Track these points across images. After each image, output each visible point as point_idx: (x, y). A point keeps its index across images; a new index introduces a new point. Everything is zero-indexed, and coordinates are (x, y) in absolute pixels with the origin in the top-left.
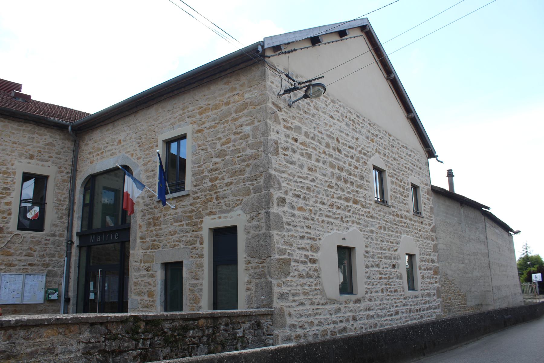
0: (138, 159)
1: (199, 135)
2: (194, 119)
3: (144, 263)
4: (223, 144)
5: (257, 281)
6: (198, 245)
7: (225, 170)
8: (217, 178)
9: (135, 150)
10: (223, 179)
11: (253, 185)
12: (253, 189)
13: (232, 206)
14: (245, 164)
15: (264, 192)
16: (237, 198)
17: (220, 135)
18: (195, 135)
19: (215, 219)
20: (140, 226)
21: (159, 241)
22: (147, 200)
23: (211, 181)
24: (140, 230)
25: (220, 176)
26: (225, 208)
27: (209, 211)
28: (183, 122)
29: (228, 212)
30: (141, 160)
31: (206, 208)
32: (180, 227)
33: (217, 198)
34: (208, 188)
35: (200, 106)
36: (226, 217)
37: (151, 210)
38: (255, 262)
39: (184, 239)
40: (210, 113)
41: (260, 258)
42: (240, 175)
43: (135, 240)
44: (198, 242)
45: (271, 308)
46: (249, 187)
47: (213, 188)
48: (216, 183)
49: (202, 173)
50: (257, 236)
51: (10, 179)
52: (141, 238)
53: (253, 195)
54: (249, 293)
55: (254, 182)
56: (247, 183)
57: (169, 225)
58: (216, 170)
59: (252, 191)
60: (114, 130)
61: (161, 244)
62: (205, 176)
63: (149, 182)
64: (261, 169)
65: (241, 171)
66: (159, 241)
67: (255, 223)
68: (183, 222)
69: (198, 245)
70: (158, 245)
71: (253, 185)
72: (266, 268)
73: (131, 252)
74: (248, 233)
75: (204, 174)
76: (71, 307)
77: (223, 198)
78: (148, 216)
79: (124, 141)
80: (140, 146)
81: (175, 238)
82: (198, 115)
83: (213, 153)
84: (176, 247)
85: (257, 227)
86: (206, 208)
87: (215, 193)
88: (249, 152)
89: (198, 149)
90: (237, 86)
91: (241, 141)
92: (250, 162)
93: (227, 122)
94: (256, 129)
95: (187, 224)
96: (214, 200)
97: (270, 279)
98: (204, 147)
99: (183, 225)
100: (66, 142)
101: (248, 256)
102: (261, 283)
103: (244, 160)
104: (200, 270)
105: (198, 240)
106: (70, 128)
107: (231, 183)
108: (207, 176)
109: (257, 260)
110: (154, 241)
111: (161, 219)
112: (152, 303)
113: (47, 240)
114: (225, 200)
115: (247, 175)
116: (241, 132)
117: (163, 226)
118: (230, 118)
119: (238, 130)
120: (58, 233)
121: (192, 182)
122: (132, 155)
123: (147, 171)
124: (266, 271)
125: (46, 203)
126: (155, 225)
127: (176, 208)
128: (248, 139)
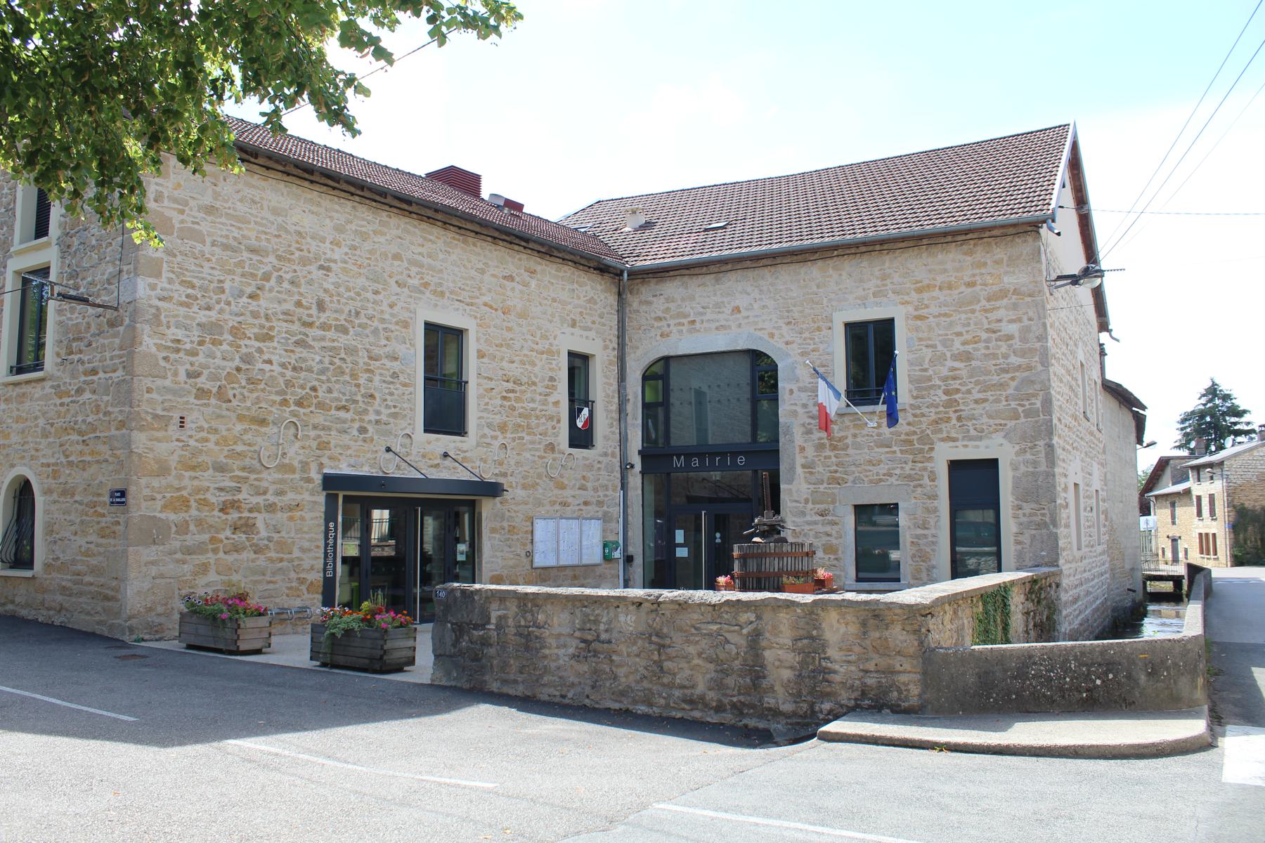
0: (787, 343)
1: (919, 323)
2: (906, 298)
4: (964, 344)
5: (1033, 532)
7: (973, 380)
8: (958, 391)
9: (779, 328)
11: (1023, 406)
12: (1023, 411)
13: (986, 431)
14: (1010, 375)
15: (1042, 417)
16: (997, 422)
17: (959, 329)
18: (910, 322)
20: (802, 449)
23: (946, 393)
25: (964, 389)
26: (973, 432)
27: (945, 435)
28: (885, 299)
29: (980, 438)
30: (794, 346)
31: (940, 431)
33: (959, 419)
35: (918, 279)
36: (977, 447)
38: (1027, 508)
40: (936, 293)
41: (1037, 502)
43: (792, 469)
44: (926, 478)
45: (1058, 566)
47: (948, 404)
48: (957, 396)
49: (930, 381)
51: (554, 362)
52: (804, 466)
53: (1023, 420)
54: (1019, 547)
55: (1026, 403)
56: (1012, 403)
57: (866, 450)
58: (954, 378)
62: (934, 385)
64: (1038, 386)
65: (1001, 385)
67: (1028, 456)
69: (926, 481)
71: (1023, 406)
72: (1048, 515)
74: (1015, 469)
76: (637, 569)
77: (971, 419)
79: (747, 309)
80: (789, 323)
81: (883, 469)
82: (913, 292)
83: (948, 354)
85: (1035, 464)
87: (956, 411)
88: (1015, 360)
90: (989, 261)
91: (999, 343)
92: (1017, 374)
93: (973, 311)
94: (1025, 331)
96: (954, 421)
97: (1054, 531)
98: (930, 342)
99: (895, 452)
100: (607, 295)
101: (1017, 499)
102: (1041, 534)
103: (1007, 372)
105: (926, 474)
106: (625, 275)
107: (985, 400)
108: (940, 387)
109: (1034, 506)
110: (836, 472)
111: (849, 441)
112: (836, 562)
113: (599, 462)
114: (974, 422)
115: (1010, 391)
116: (1000, 331)
117: (850, 451)
118: (977, 307)
119: (994, 326)
120: (610, 452)
121: (910, 391)
122: (772, 335)
124: (1047, 520)
125: (467, 382)
128: (1011, 342)
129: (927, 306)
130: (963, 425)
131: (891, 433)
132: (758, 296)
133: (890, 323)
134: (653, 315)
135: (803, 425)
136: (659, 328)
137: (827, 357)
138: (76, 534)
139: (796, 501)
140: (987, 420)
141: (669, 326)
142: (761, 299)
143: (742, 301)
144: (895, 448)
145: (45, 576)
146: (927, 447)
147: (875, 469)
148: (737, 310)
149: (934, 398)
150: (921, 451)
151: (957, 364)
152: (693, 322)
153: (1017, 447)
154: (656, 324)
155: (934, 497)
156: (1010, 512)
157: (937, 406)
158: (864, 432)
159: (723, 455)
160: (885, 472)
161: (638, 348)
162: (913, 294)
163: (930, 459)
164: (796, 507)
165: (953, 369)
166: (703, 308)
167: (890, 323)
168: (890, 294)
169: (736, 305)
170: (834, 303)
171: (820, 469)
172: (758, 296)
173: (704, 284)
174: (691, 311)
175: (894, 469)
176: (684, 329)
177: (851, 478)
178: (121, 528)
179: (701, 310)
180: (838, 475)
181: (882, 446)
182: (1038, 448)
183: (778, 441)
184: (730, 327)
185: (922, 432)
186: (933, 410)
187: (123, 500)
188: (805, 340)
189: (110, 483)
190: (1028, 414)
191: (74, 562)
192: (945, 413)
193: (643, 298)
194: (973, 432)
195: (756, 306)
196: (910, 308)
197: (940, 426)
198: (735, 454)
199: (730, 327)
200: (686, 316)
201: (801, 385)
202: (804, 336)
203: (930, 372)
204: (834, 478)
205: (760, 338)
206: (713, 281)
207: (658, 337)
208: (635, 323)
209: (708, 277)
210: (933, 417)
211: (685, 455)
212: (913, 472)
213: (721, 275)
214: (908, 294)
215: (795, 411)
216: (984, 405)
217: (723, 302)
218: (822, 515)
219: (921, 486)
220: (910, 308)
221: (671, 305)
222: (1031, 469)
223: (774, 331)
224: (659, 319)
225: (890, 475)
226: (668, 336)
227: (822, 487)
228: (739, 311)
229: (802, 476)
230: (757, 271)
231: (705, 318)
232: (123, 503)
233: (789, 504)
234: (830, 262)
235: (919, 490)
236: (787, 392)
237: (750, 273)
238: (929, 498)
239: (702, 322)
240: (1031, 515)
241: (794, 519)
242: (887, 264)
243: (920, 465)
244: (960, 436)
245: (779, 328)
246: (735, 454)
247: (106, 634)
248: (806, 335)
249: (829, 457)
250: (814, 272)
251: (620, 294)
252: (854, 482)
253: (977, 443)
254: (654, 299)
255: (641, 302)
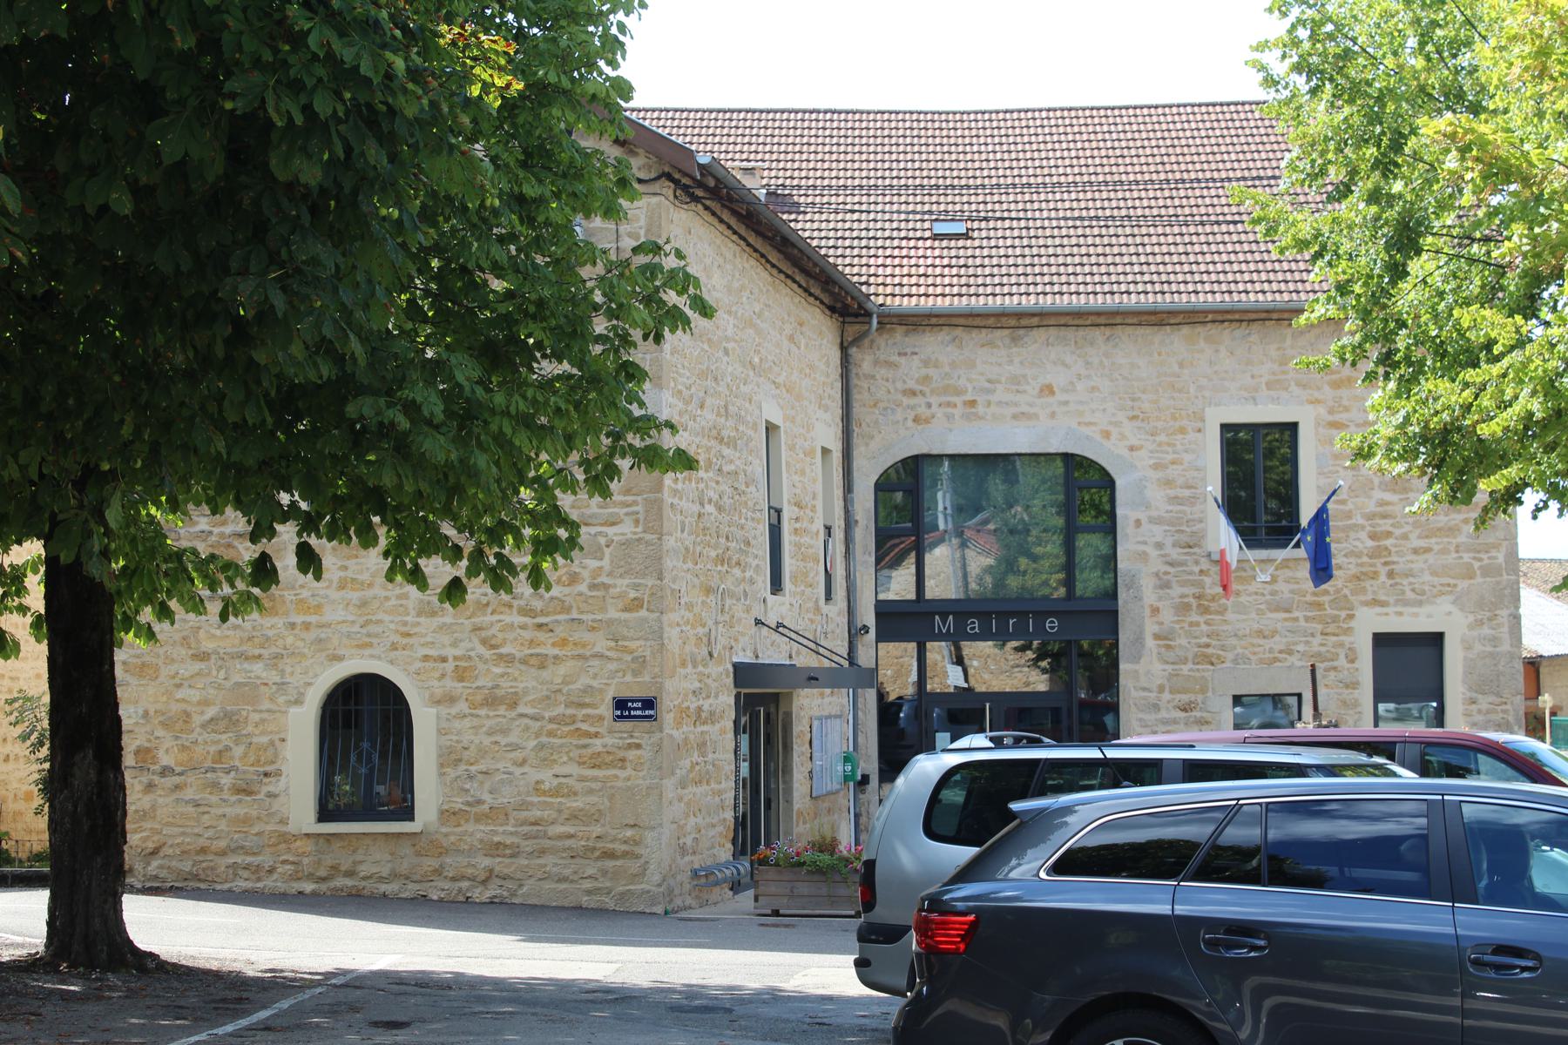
2: (1317, 395)
3: (1171, 692)
6: (1342, 662)
8: (1389, 534)
9: (1117, 424)
10: (1405, 537)
11: (1480, 560)
15: (1505, 577)
18: (1321, 430)
19: (1387, 614)
20: (1155, 611)
21: (1223, 648)
22: (1175, 553)
23: (1373, 536)
24: (1155, 619)
25: (1397, 532)
26: (1410, 595)
27: (1370, 597)
29: (1420, 604)
30: (1143, 453)
31: (1364, 591)
32: (1287, 624)
33: (1391, 574)
34: (1365, 551)
36: (1416, 615)
37: (1191, 577)
38: (1484, 702)
39: (1301, 648)
41: (1498, 695)
42: (1447, 536)
43: (1139, 640)
44: (1342, 656)
46: (1472, 565)
47: (1376, 553)
48: (1389, 542)
49: (1350, 518)
50: (1492, 655)
52: (1157, 637)
53: (1479, 580)
55: (1484, 556)
57: (1253, 615)
58: (1384, 516)
59: (1478, 572)
60: (1015, 349)
61: (1230, 656)
62: (1355, 525)
63: (1180, 512)
65: (1450, 529)
66: (1223, 648)
67: (1486, 631)
68: (1296, 614)
69: (1342, 662)
70: (1219, 657)
71: (1480, 560)
72: (1512, 713)
73: (1123, 666)
74: (1468, 648)
75: (1354, 521)
77: (1407, 576)
78: (1177, 591)
79: (1065, 391)
80: (1134, 418)
81: (1278, 643)
84: (1278, 664)
85: (1494, 641)
86: (1364, 591)
87: (1386, 564)
89: (1331, 462)
95: (1307, 619)
96: (1383, 578)
99: (1296, 619)
101: (1470, 689)
104: (1351, 712)
107: (1428, 550)
108: (1363, 527)
109: (1491, 698)
110: (1208, 646)
114: (1411, 579)
115: (1462, 539)
117: (1230, 616)
122: (1107, 435)
123: (1168, 483)
124: (1511, 719)
126: (1205, 610)
127: (1274, 580)
129: (1347, 409)
130: (1396, 584)
131: (1292, 592)
132: (1083, 372)
133: (1293, 427)
134: (899, 385)
135: (1157, 575)
136: (912, 408)
137: (1195, 474)
138: (523, 762)
139: (1144, 689)
140: (1430, 578)
141: (929, 405)
142: (1088, 377)
143: (1058, 378)
144: (1296, 614)
145: (444, 830)
146: (1343, 614)
147: (1267, 644)
148: (1048, 390)
149: (1357, 543)
150: (1335, 619)
151: (1388, 496)
152: (973, 403)
153: (1471, 618)
154: (906, 401)
155: (1354, 685)
156: (1461, 708)
157: (1359, 555)
158: (1252, 588)
159: (1022, 615)
160: (1283, 647)
161: (872, 437)
162: (1327, 388)
163: (1348, 631)
164: (1145, 698)
165: (1382, 503)
166: (989, 381)
167: (1293, 427)
168: (1293, 388)
169: (1047, 382)
170: (1207, 394)
171: (1183, 641)
172: (1083, 372)
173: (991, 344)
174: (968, 385)
175: (1295, 644)
176: (957, 412)
177: (1230, 656)
178: (646, 753)
179: (987, 385)
180: (1210, 651)
181: (1277, 609)
182: (1500, 620)
183: (1113, 595)
184: (1036, 416)
185: (1338, 591)
186: (1352, 560)
187: (651, 712)
188: (1160, 444)
189: (613, 686)
190: (1487, 571)
191: (524, 806)
192: (1371, 565)
193: (882, 357)
194: (1410, 595)
195: (1080, 386)
196: (1322, 410)
197: (1363, 584)
198: (1042, 615)
199: (1036, 416)
200: (959, 392)
201: (1154, 513)
202: (1158, 439)
203: (1350, 506)
204: (1205, 656)
205: (1088, 437)
206: (1007, 341)
207: (910, 423)
208: (866, 395)
209: (999, 333)
210: (1353, 570)
211: (954, 614)
212: (1323, 649)
213: (1022, 332)
214: (1319, 389)
215: (1144, 553)
216: (1426, 556)
217: (1024, 376)
218: (1185, 710)
219: (1335, 668)
220: (1322, 410)
221: (932, 372)
222: (1489, 649)
223: (1110, 428)
224: (913, 393)
225: (1290, 652)
226: (927, 421)
227: (1185, 669)
228: (1052, 393)
229: (1155, 651)
230: (1081, 332)
231: (994, 398)
232: (651, 716)
233: (1134, 693)
234: (1199, 329)
235: (1332, 674)
236: (1132, 523)
237: (1070, 333)
238: (1347, 687)
239: (989, 404)
240: (1488, 712)
241: (1141, 715)
242: (1289, 342)
243: (1334, 639)
244: (1391, 600)
245: (1117, 424)
246: (1042, 615)
247: (611, 905)
248: (1162, 438)
249: (1197, 624)
250: (1175, 342)
251: (844, 349)
252: (1235, 661)
253: (1415, 610)
254: (903, 360)
255: (876, 363)
